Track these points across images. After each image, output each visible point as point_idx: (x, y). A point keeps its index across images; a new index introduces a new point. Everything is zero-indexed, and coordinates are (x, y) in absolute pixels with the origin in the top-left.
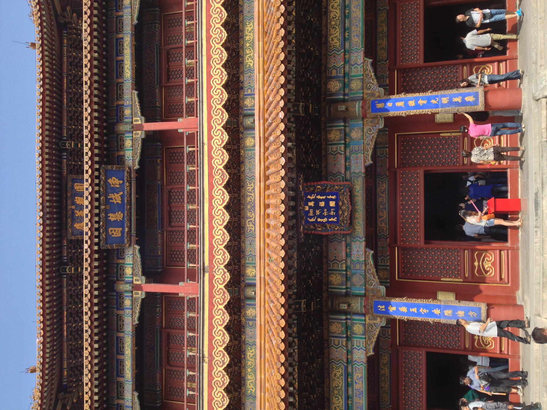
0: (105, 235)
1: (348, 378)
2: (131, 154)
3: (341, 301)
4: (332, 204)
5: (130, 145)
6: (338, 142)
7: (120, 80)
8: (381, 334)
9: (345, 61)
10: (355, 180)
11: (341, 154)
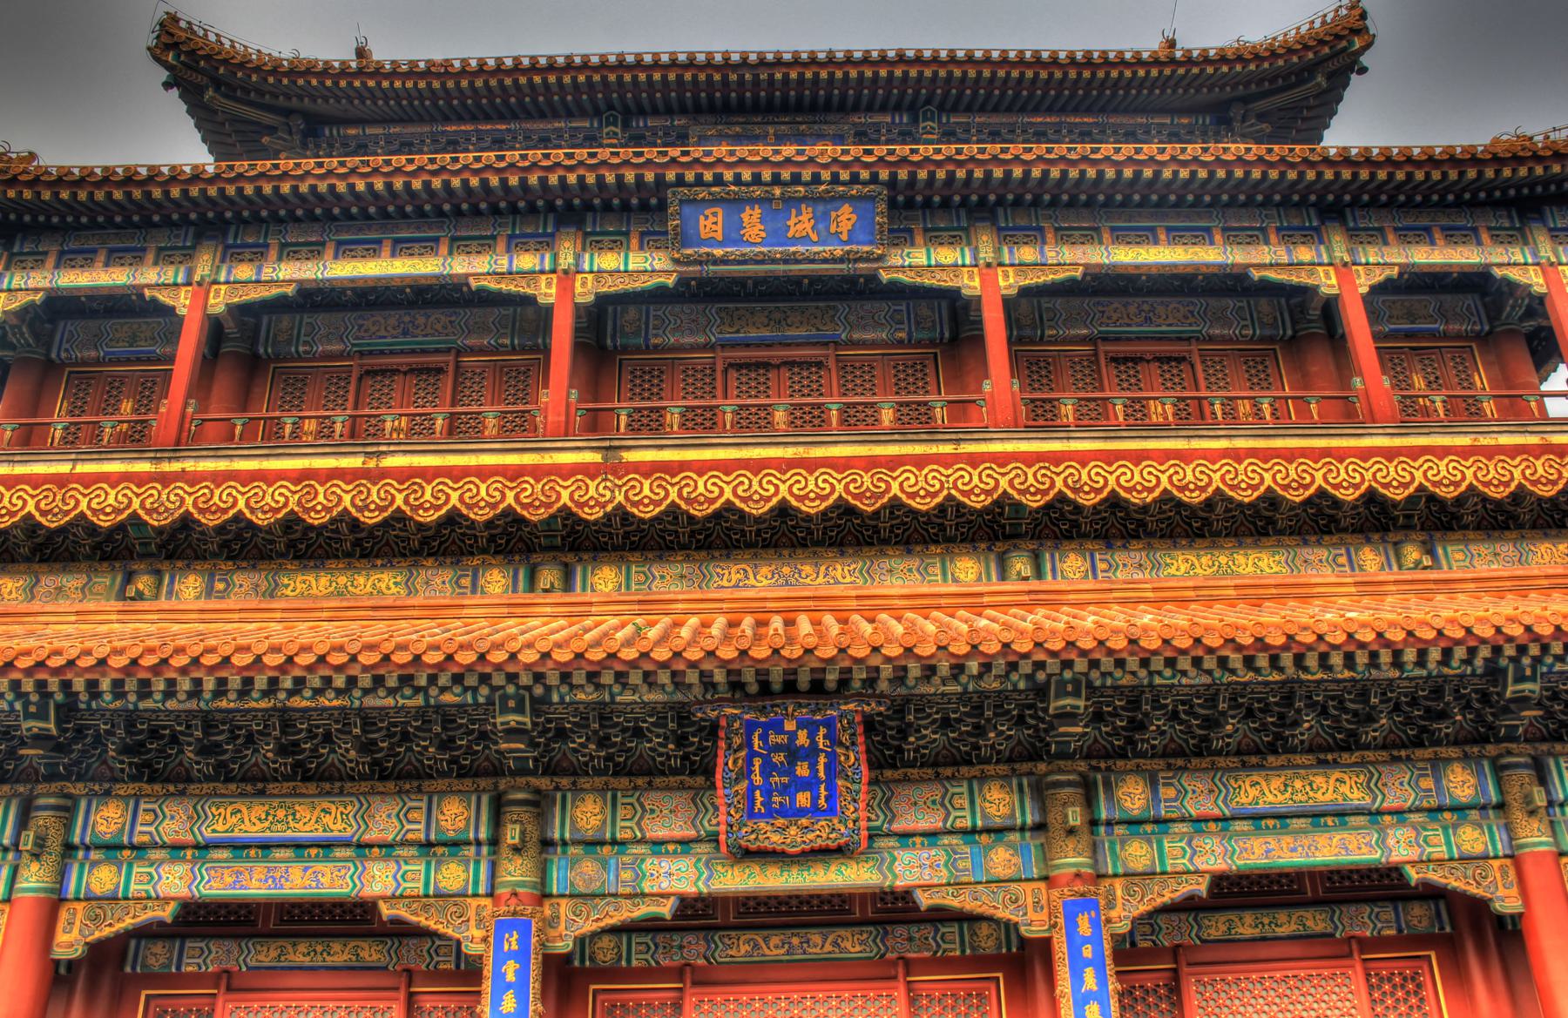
0: (703, 200)
1: (319, 846)
3: (529, 828)
4: (803, 799)
5: (943, 261)
6: (978, 810)
7: (1106, 236)
8: (438, 943)
9: (1198, 820)
10: (871, 863)
11: (945, 820)
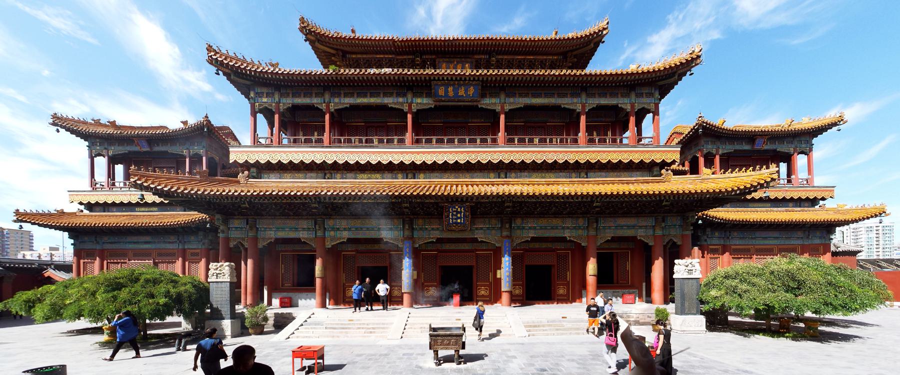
2: (489, 102)
